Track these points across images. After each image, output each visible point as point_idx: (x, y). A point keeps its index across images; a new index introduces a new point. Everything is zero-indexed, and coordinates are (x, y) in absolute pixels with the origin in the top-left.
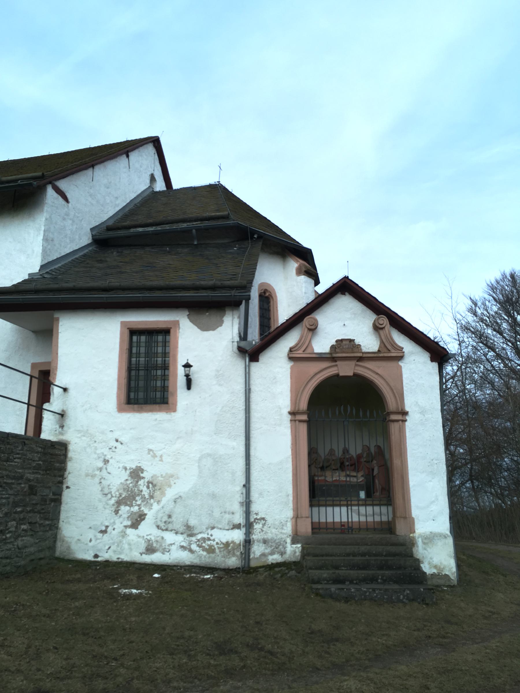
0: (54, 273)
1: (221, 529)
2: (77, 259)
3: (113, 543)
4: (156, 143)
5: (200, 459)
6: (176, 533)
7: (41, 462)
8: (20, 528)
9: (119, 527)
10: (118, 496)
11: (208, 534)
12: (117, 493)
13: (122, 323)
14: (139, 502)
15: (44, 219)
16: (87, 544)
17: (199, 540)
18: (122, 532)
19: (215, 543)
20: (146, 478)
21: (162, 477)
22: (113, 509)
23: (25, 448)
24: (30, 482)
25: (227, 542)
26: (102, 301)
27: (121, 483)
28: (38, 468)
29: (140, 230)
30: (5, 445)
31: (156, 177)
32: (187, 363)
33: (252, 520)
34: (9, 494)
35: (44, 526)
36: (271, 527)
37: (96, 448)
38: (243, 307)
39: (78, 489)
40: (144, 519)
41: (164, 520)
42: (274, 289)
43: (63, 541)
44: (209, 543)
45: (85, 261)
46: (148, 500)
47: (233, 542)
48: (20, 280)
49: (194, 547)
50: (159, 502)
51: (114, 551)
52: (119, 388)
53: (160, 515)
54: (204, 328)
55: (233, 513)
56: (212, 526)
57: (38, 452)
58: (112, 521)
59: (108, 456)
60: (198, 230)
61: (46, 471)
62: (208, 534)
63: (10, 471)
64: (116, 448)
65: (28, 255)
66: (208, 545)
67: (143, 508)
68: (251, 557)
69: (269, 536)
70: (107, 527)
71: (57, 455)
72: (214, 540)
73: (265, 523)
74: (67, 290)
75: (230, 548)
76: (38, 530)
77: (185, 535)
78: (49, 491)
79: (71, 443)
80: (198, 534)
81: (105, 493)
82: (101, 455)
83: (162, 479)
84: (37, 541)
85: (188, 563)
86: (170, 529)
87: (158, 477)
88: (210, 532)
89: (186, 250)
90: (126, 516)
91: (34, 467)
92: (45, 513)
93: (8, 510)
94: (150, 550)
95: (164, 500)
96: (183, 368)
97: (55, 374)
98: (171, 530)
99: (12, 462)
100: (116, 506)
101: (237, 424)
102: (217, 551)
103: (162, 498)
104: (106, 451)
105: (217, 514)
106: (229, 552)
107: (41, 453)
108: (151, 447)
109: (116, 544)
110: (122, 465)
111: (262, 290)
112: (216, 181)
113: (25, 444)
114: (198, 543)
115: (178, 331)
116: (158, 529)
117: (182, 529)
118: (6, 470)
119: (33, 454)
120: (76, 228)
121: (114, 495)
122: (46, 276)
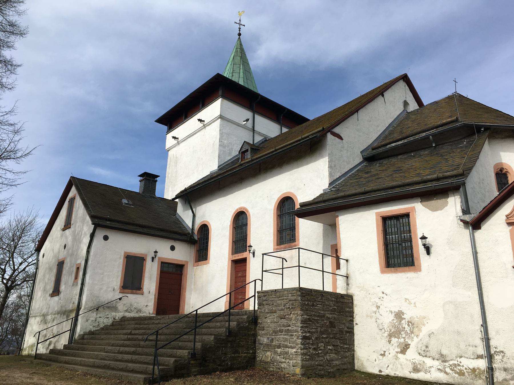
0: (338, 187)
1: (467, 358)
2: (353, 174)
3: (391, 363)
4: (405, 78)
5: (444, 305)
6: (433, 359)
7: (335, 307)
8: (327, 348)
9: (393, 353)
11: (458, 362)
12: (388, 329)
13: (376, 213)
14: (404, 336)
15: (328, 155)
16: (373, 363)
17: (451, 365)
18: (395, 356)
19: (464, 368)
20: (406, 319)
21: (417, 318)
22: (387, 340)
23: (324, 298)
24: (330, 319)
25: (474, 368)
26: (361, 201)
27: (390, 322)
28: (334, 311)
29: (393, 145)
30: (310, 296)
32: (423, 236)
33: (492, 352)
34: (317, 326)
35: (344, 348)
36: (510, 359)
38: (461, 189)
39: (363, 326)
40: (409, 348)
41: (423, 349)
42: (510, 166)
43: (358, 359)
44: (459, 368)
45: (357, 175)
46: (410, 334)
47: (478, 368)
48: (318, 195)
49: (448, 370)
50: (417, 336)
51: (392, 369)
52: (380, 257)
53: (420, 346)
54: (434, 209)
55: (476, 347)
56: (460, 355)
57: (332, 301)
58: (387, 348)
59: (378, 303)
60: (433, 135)
61: (340, 313)
62: (458, 362)
64: (383, 298)
65: (322, 178)
66: (459, 370)
67: (407, 340)
68: (495, 381)
69: (508, 366)
70: (385, 352)
71: (346, 302)
72: (463, 366)
73: (504, 355)
75: (476, 373)
76: (340, 350)
77: (440, 361)
78: (344, 326)
79: (355, 295)
80: (450, 361)
81: (380, 328)
82: (374, 303)
83: (418, 320)
84: (340, 357)
85: (445, 382)
86: (428, 356)
87: (415, 318)
88: (459, 360)
89: (427, 152)
90: (396, 345)
93: (318, 336)
94: (416, 370)
95: (421, 335)
96: (420, 239)
97: (341, 251)
98: (430, 357)
99: (316, 307)
100: (388, 338)
101: (470, 278)
102: (466, 374)
103: (419, 333)
104: (377, 300)
105: (463, 346)
106: (476, 376)
108: (406, 298)
109: (392, 364)
110: (389, 309)
111: (497, 169)
112: (453, 92)
113: (323, 296)
114: (450, 367)
115: (415, 214)
116: (420, 355)
117: (437, 356)
118: (313, 311)
120: (350, 154)
121: (386, 330)
122: (332, 189)
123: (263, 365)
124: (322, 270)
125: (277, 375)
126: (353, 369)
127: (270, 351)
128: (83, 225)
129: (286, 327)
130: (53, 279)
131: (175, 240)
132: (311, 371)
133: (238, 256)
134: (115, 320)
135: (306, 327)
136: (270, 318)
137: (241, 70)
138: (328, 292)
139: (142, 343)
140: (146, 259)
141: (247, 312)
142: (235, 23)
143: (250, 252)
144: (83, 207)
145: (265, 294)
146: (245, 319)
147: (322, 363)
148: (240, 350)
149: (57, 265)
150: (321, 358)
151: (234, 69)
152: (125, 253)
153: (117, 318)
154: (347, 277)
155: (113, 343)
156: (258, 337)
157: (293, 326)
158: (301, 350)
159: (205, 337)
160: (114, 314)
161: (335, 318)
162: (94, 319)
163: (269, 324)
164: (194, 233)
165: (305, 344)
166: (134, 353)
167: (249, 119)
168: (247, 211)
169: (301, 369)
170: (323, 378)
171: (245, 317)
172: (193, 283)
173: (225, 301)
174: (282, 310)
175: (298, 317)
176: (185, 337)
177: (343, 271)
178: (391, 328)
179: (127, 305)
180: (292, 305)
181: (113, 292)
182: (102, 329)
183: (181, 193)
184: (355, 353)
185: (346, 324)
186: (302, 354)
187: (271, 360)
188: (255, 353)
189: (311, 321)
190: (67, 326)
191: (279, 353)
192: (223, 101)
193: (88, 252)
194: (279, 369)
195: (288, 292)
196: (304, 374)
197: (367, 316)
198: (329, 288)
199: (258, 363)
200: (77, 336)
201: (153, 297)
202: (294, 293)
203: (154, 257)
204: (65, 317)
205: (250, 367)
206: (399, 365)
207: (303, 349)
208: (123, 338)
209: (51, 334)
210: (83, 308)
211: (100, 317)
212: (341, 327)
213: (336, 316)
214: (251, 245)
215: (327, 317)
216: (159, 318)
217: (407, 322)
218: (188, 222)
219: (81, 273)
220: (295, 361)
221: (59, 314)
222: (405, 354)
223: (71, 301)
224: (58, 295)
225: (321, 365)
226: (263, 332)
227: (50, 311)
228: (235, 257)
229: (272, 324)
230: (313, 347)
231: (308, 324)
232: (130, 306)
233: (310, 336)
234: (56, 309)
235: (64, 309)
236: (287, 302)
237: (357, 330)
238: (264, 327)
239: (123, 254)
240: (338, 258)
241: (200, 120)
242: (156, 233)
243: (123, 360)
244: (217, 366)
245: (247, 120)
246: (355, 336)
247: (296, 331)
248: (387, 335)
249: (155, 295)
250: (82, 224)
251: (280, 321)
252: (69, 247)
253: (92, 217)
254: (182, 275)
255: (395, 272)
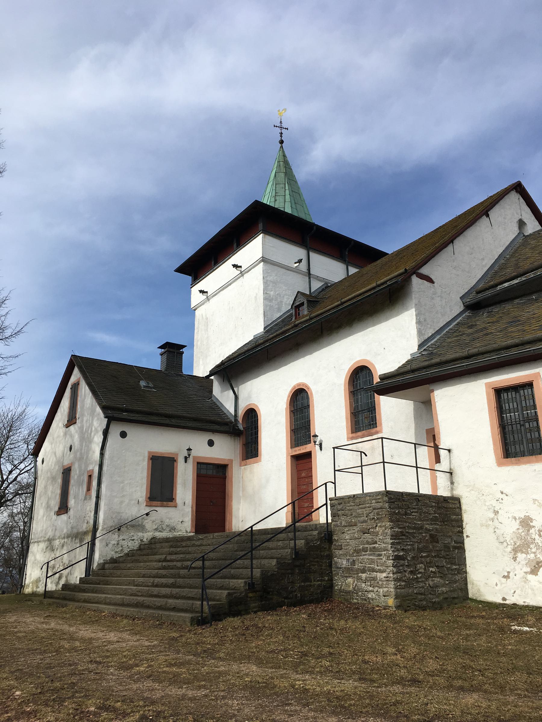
2: (451, 329)
3: (518, 588)
7: (436, 515)
8: (429, 570)
10: (513, 544)
12: (512, 542)
13: (486, 384)
14: (534, 550)
15: (414, 305)
16: (493, 588)
18: (523, 577)
20: (536, 527)
22: (511, 556)
24: (430, 532)
27: (514, 532)
28: (435, 519)
29: (506, 285)
31: (525, 221)
34: (413, 542)
37: (485, 501)
39: (477, 538)
43: (473, 584)
45: (457, 330)
48: (404, 362)
57: (432, 507)
58: (512, 567)
59: (496, 507)
61: (443, 522)
63: (410, 523)
64: (502, 499)
67: (538, 556)
70: (509, 572)
71: (451, 508)
74: (436, 364)
76: (447, 573)
82: (491, 507)
84: (447, 582)
90: (524, 562)
91: (431, 519)
92: (450, 558)
97: (440, 438)
99: (410, 515)
100: (513, 553)
104: (494, 503)
107: (435, 507)
108: (535, 497)
109: (520, 589)
110: (512, 515)
113: (419, 500)
118: (406, 522)
119: (428, 508)
120: (446, 302)
121: (509, 543)
123: (343, 595)
124: (415, 466)
125: (362, 608)
126: (466, 597)
127: (352, 577)
128: (93, 420)
129: (370, 544)
130: (58, 491)
131: (214, 431)
132: (409, 602)
133: (300, 450)
134: (143, 543)
135: (398, 543)
136: (349, 533)
137: (287, 192)
138: (425, 495)
139: (182, 572)
140: (177, 459)
141: (318, 526)
142: (274, 126)
143: (315, 444)
144: (91, 394)
145: (340, 502)
146: (315, 535)
147: (422, 590)
148: (312, 577)
149: (63, 473)
150: (421, 585)
151: (277, 191)
152: (149, 453)
153: (145, 540)
154: (451, 473)
155: (143, 573)
156: (335, 559)
157: (381, 542)
158: (393, 574)
159: (265, 562)
160: (140, 534)
161: (437, 530)
162: (116, 543)
163: (348, 541)
164: (238, 421)
165: (399, 566)
166: (173, 586)
167: (302, 259)
168: (308, 388)
169: (396, 598)
170: (425, 610)
171: (315, 533)
172: (241, 489)
173: (286, 511)
174: (365, 521)
175: (386, 531)
176: (238, 562)
177: (444, 465)
178: (515, 540)
179: (157, 522)
180: (378, 514)
181: (137, 505)
182: (127, 555)
183: (217, 368)
184: (468, 576)
185: (453, 536)
186: (395, 580)
187: (354, 588)
188: (331, 580)
189: (404, 535)
190: (82, 553)
191: (364, 579)
192: (265, 237)
193: (102, 454)
194: (366, 600)
195: (371, 497)
196: (399, 606)
197: (482, 525)
198: (426, 490)
199: (336, 593)
200: (95, 565)
201: (190, 509)
202: (379, 499)
203: (188, 456)
204: (77, 541)
205: (326, 599)
206: (530, 590)
207: (397, 572)
208: (156, 566)
209: (61, 565)
210: (100, 528)
211: (124, 540)
212: (446, 542)
213: (438, 527)
214: (317, 434)
215: (426, 529)
216: (201, 537)
217: (538, 531)
218: (230, 407)
219: (95, 483)
220: (386, 589)
221: (70, 538)
222: (537, 575)
223: (84, 520)
224: (67, 513)
225: (421, 594)
226: (341, 552)
227: (58, 534)
228: (295, 451)
229: (351, 541)
230: (409, 570)
231: (401, 539)
232: (161, 523)
233: (404, 555)
234: (65, 531)
235: (75, 531)
236: (370, 511)
237: (468, 544)
238: (341, 545)
239: (146, 455)
240: (436, 448)
241: (236, 266)
242: (187, 424)
243: (160, 594)
244: (283, 599)
245: (300, 261)
246: (466, 552)
247: (385, 549)
248: (511, 549)
249: (192, 508)
250: (91, 418)
251: (362, 537)
252: (76, 448)
253: (104, 408)
254: (225, 478)
255: (517, 464)
